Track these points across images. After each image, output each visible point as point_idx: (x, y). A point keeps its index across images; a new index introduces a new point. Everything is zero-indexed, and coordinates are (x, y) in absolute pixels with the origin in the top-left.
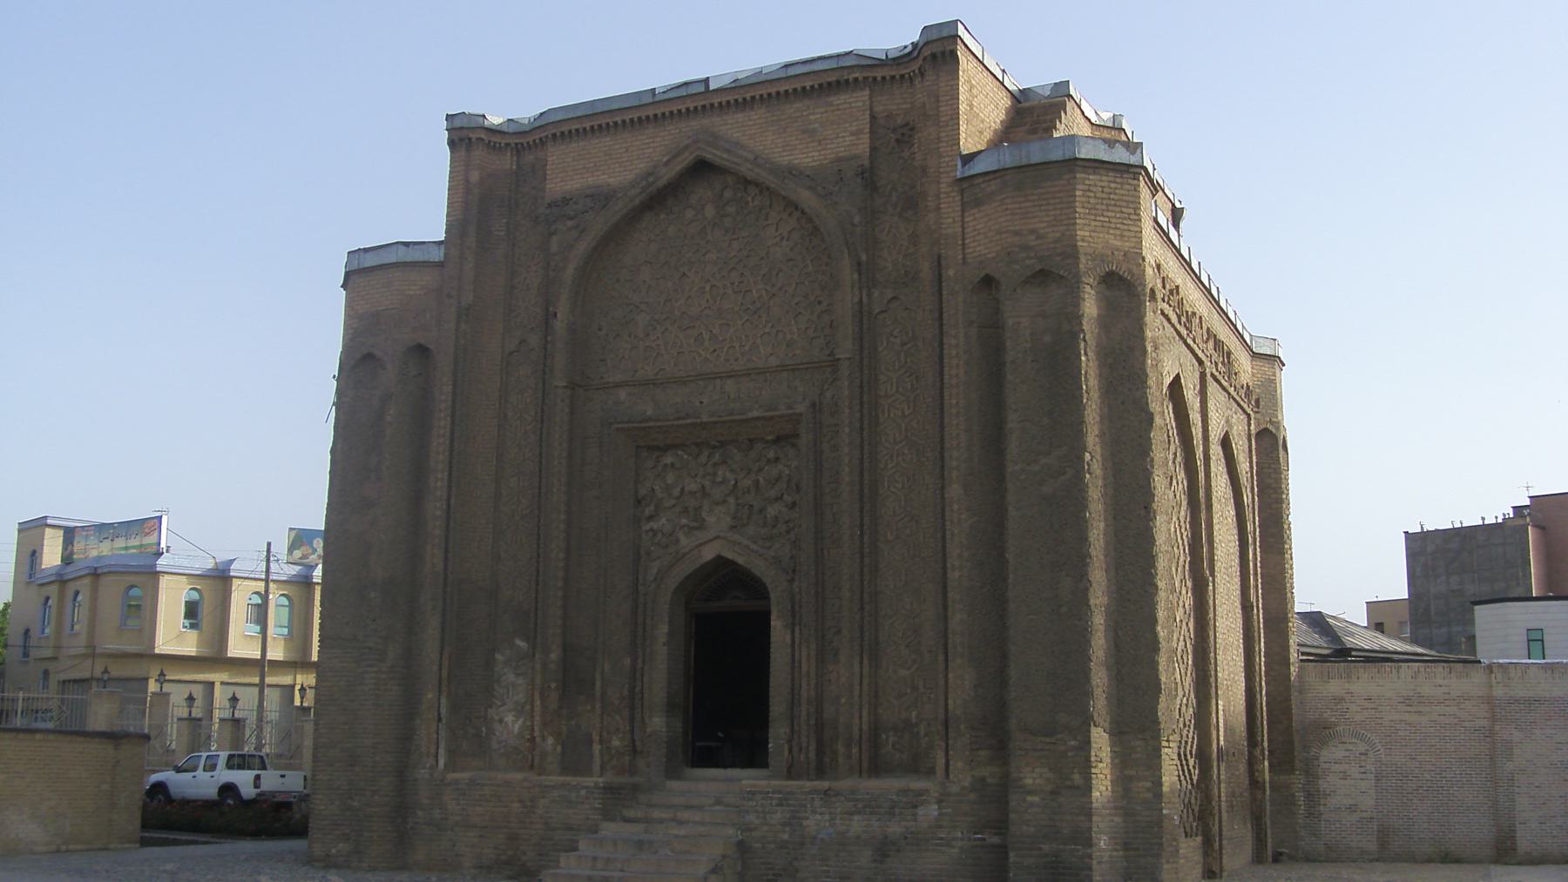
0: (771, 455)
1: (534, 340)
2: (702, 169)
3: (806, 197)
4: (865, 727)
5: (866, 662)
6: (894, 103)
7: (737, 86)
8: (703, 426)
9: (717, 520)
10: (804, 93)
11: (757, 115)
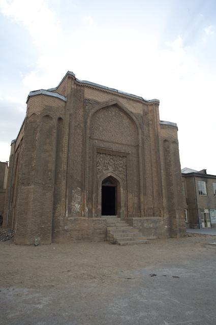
0: (121, 159)
1: (82, 125)
2: (116, 105)
7: (122, 94)
9: (111, 169)
10: (133, 100)
11: (125, 100)
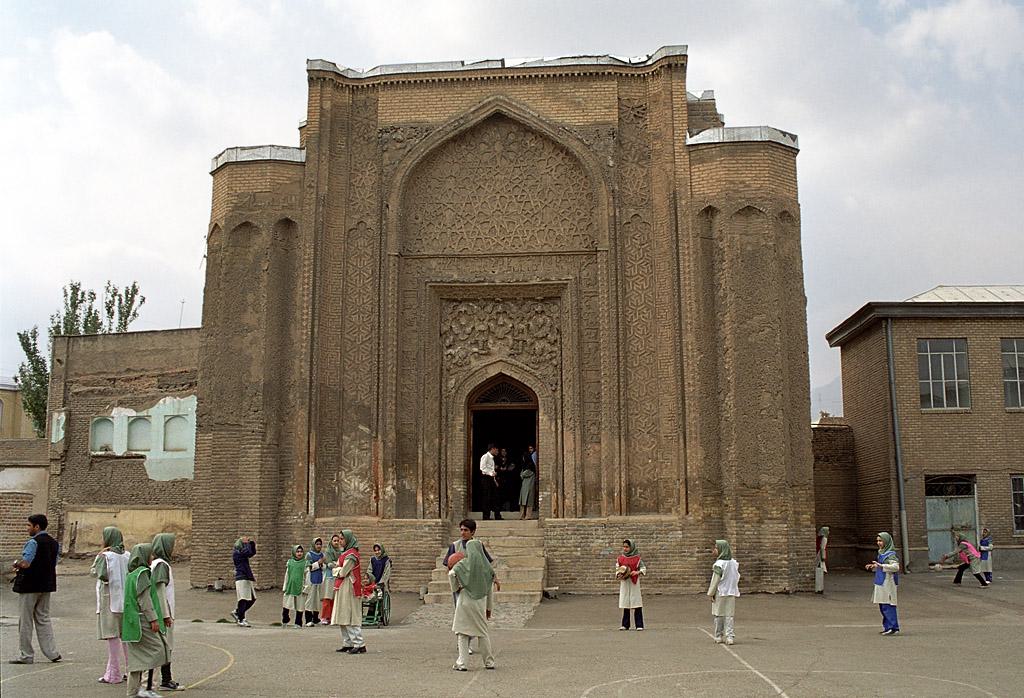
0: (539, 309)
3: (575, 147)
4: (623, 484)
5: (623, 443)
6: (634, 91)
8: (495, 287)
9: (499, 350)
11: (539, 87)
